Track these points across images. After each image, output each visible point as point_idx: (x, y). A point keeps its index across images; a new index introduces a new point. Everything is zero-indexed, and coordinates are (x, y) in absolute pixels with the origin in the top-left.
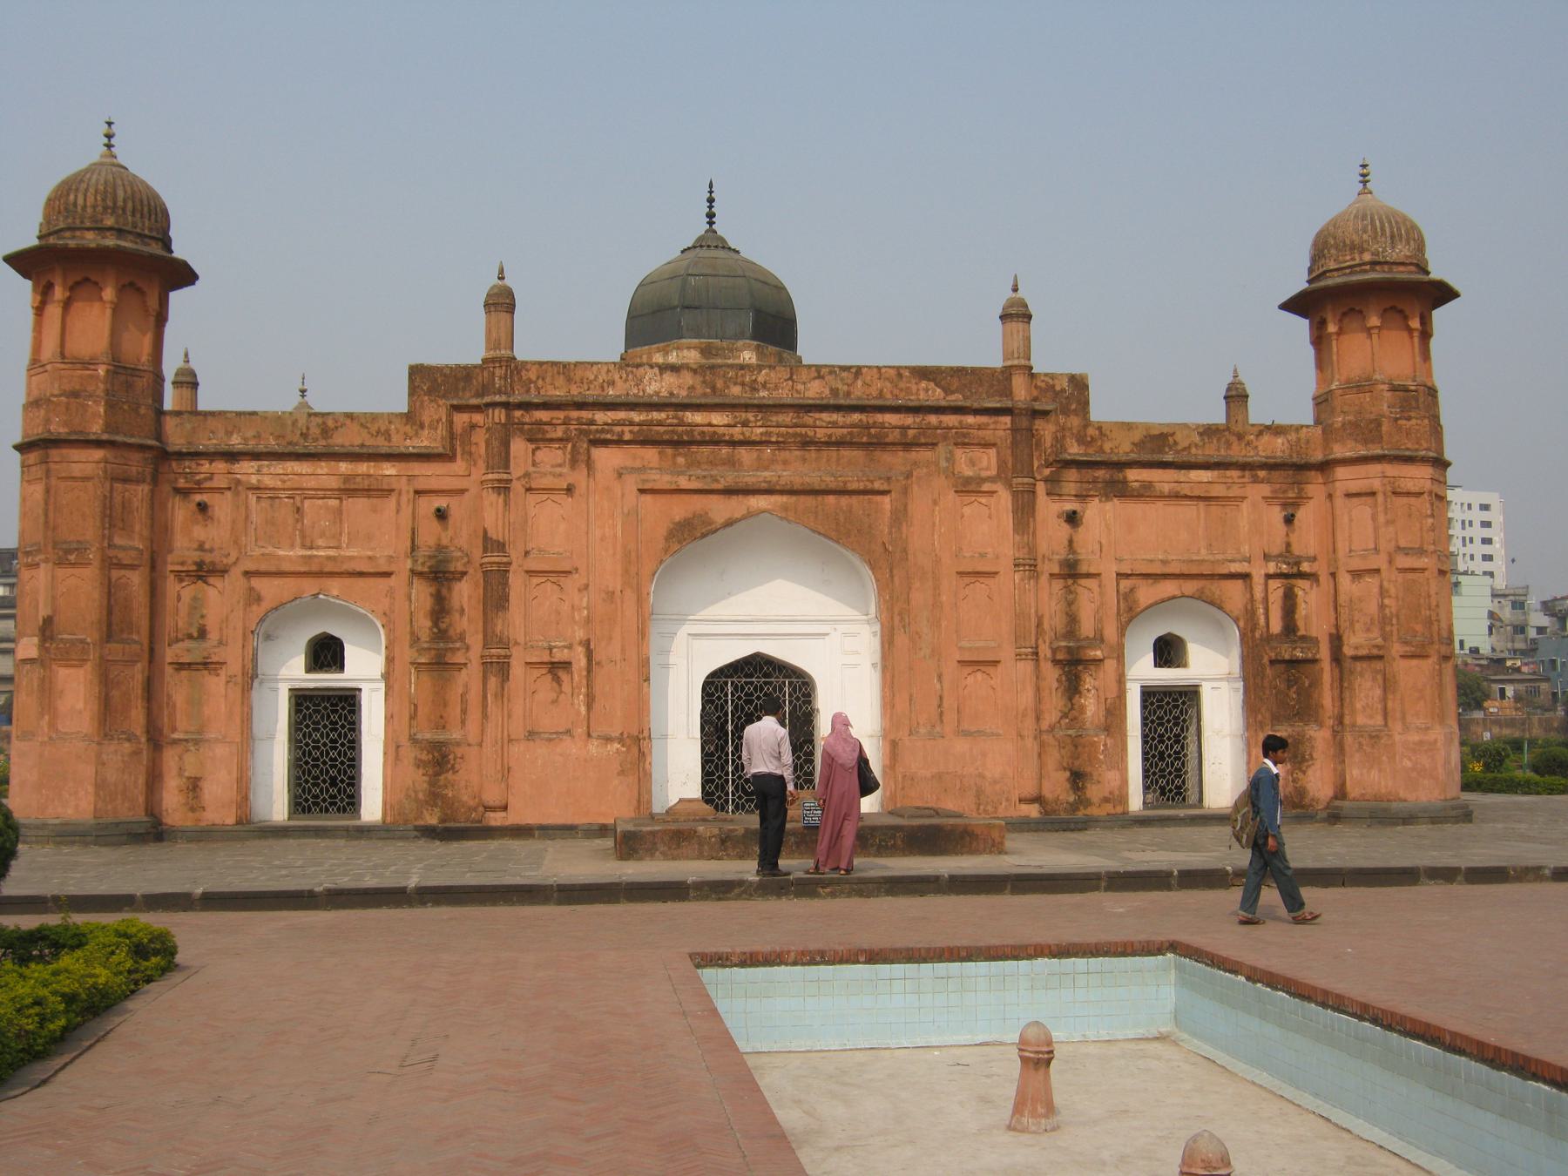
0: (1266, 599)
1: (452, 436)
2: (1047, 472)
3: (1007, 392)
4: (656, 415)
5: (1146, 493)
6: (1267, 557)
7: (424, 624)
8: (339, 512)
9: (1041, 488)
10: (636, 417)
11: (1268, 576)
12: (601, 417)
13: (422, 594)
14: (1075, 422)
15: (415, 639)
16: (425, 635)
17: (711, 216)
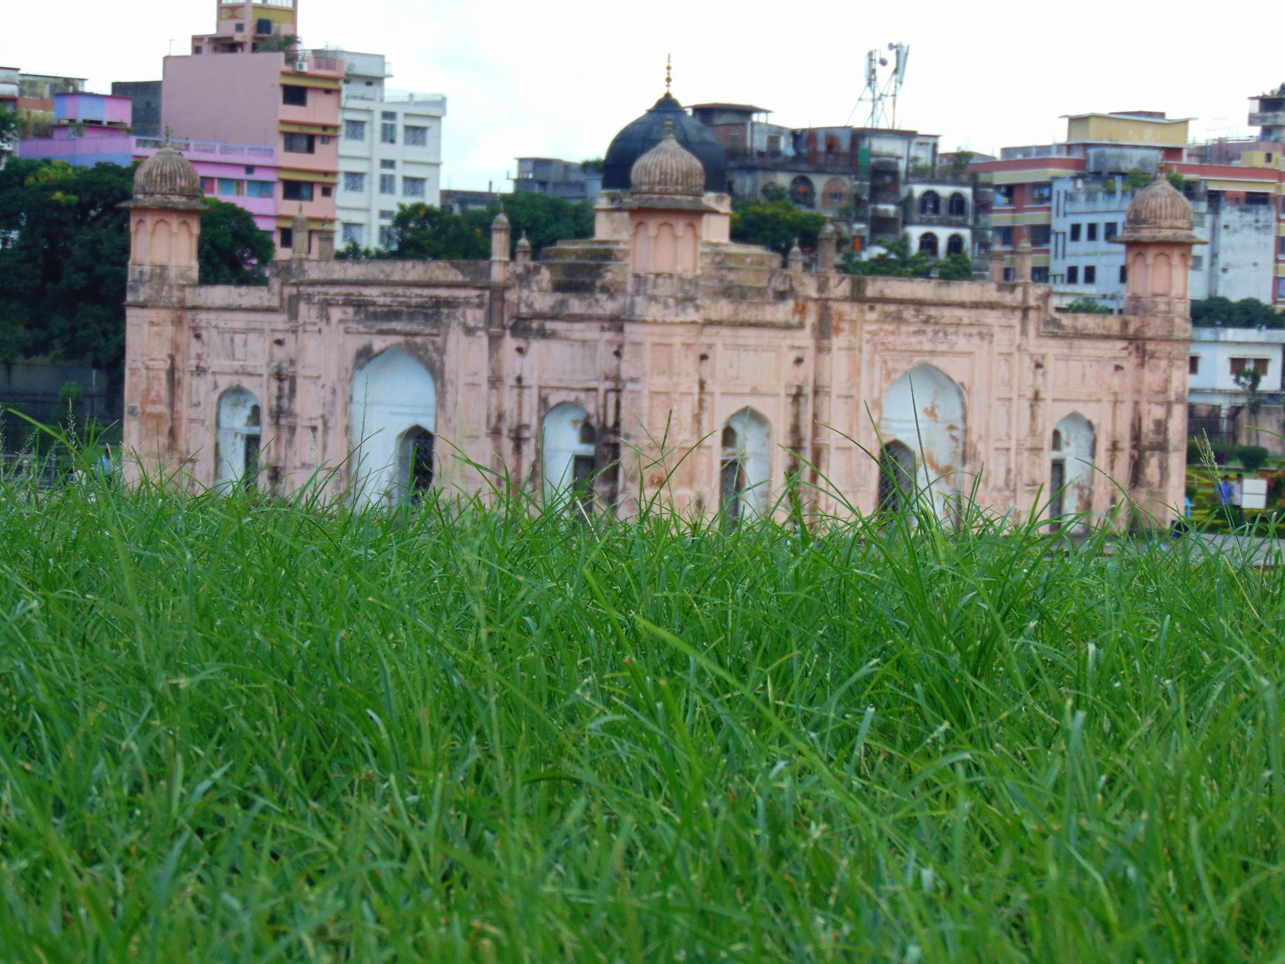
0: (605, 406)
1: (282, 300)
2: (511, 323)
3: (489, 276)
4: (354, 290)
5: (553, 335)
6: (607, 378)
7: (274, 403)
8: (246, 342)
9: (508, 332)
10: (344, 290)
11: (607, 391)
12: (333, 290)
13: (274, 384)
14: (525, 293)
15: (271, 411)
16: (275, 409)
17: (669, 80)
